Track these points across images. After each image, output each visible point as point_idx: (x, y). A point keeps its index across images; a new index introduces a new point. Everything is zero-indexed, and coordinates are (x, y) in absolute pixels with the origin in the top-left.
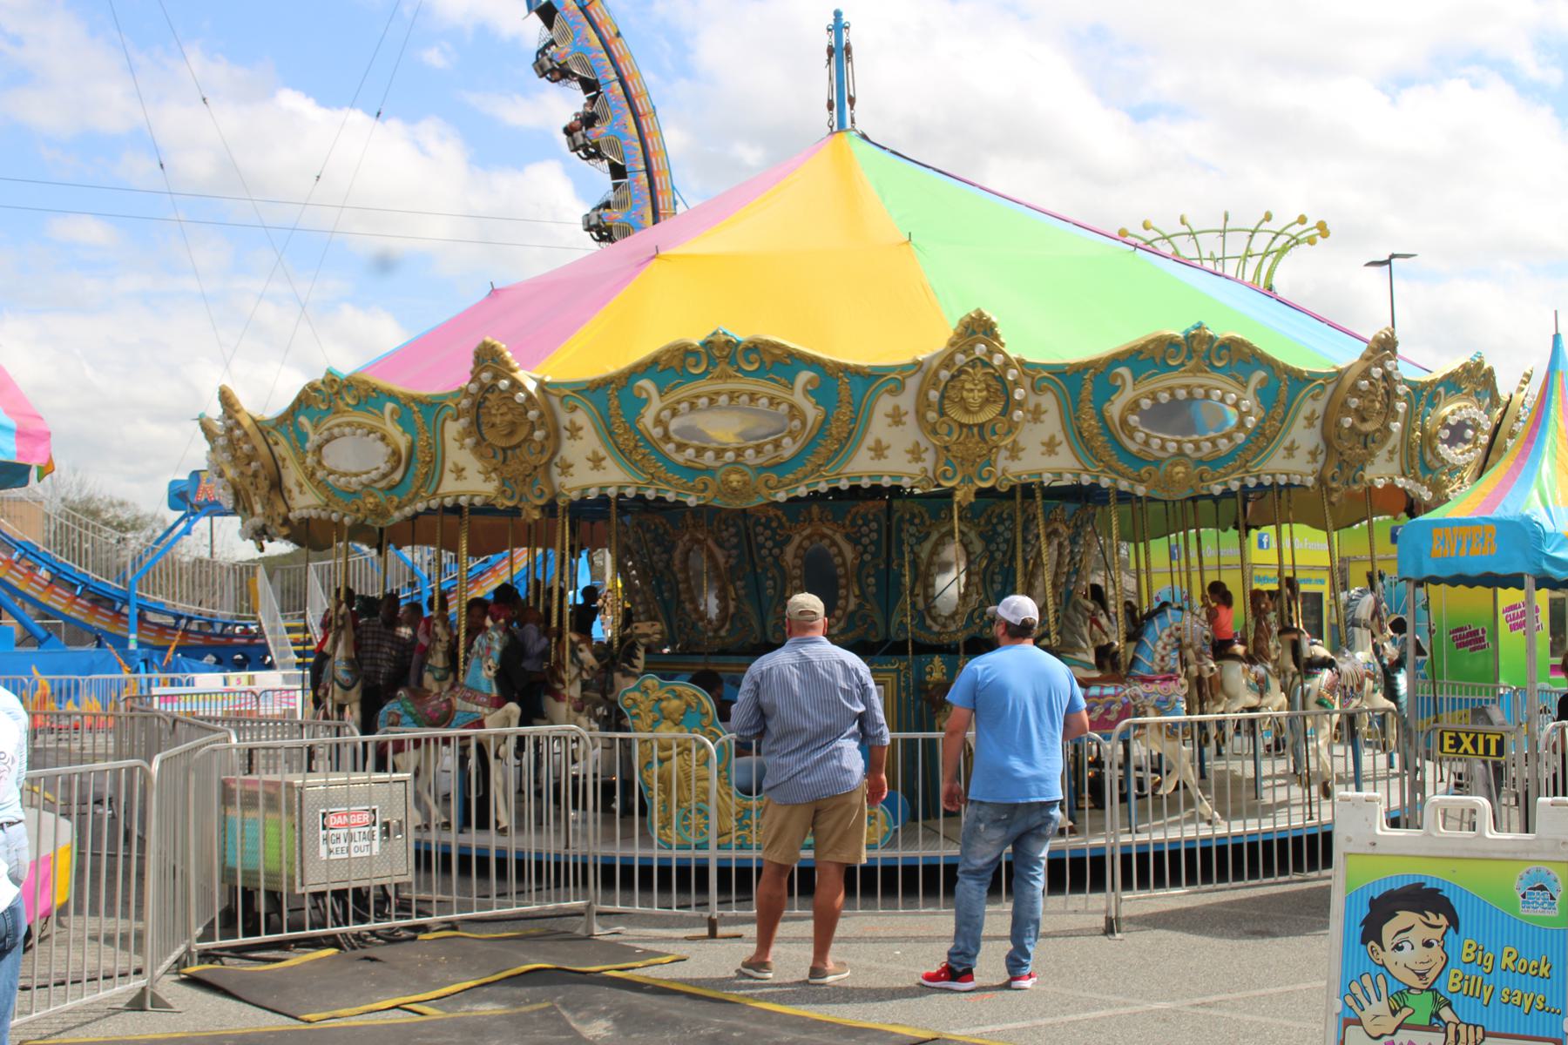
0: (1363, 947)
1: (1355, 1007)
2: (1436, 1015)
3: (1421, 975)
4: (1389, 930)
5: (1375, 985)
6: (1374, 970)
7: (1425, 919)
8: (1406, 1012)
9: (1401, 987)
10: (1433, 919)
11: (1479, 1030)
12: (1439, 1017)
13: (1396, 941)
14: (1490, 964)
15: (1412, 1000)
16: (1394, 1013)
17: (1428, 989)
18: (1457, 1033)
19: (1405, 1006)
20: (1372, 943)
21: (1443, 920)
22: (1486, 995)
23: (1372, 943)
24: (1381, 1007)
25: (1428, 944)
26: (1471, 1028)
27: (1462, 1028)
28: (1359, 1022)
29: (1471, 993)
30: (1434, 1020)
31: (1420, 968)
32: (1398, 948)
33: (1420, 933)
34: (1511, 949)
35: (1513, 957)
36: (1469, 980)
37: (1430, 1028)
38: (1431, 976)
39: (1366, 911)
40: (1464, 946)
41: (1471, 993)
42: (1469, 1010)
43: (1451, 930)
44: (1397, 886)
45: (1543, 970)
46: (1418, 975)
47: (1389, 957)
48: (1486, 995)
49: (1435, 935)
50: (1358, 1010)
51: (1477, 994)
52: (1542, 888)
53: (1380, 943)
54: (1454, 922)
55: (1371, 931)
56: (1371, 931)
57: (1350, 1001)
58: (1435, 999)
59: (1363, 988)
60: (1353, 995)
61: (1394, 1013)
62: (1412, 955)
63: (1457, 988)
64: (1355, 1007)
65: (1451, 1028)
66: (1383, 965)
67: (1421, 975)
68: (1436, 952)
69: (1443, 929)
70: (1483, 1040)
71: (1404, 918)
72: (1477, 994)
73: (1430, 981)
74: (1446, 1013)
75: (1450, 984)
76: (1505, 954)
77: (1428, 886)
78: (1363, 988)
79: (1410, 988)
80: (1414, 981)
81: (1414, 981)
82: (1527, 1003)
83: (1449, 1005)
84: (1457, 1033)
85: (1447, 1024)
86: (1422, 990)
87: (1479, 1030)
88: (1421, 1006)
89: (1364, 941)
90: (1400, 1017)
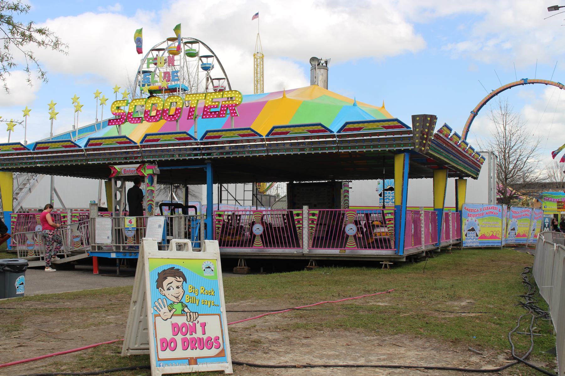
0: (157, 289)
1: (157, 310)
2: (183, 310)
3: (177, 298)
4: (165, 283)
5: (163, 302)
6: (163, 297)
7: (176, 279)
8: (174, 310)
9: (171, 302)
11: (197, 314)
12: (184, 311)
13: (168, 287)
14: (197, 292)
15: (175, 306)
16: (170, 311)
17: (180, 302)
18: (190, 315)
19: (173, 308)
20: (160, 288)
21: (181, 279)
22: (197, 302)
23: (160, 288)
24: (166, 309)
25: (178, 287)
26: (194, 313)
27: (191, 314)
28: (159, 315)
29: (193, 302)
30: (183, 312)
31: (177, 295)
32: (169, 289)
33: (175, 284)
34: (203, 287)
35: (204, 290)
36: (192, 298)
37: (182, 315)
38: (180, 298)
39: (157, 277)
40: (188, 287)
41: (193, 302)
42: (192, 307)
43: (184, 282)
45: (212, 293)
46: (176, 298)
47: (166, 292)
48: (197, 302)
49: (180, 284)
50: (158, 311)
51: (195, 303)
52: (209, 267)
53: (163, 288)
54: (185, 280)
55: (159, 284)
57: (156, 309)
58: (182, 305)
59: (159, 304)
60: (156, 306)
61: (170, 311)
62: (174, 291)
63: (188, 301)
64: (157, 310)
65: (188, 314)
66: (165, 295)
67: (177, 298)
69: (182, 282)
70: (198, 317)
71: (170, 279)
72: (195, 303)
73: (180, 299)
74: (186, 309)
76: (201, 289)
77: (176, 268)
78: (159, 304)
79: (174, 302)
80: (176, 300)
81: (176, 300)
82: (209, 304)
83: (187, 306)
84: (190, 315)
85: (187, 313)
86: (178, 303)
87: (197, 314)
88: (178, 307)
89: (158, 288)
90: (172, 312)
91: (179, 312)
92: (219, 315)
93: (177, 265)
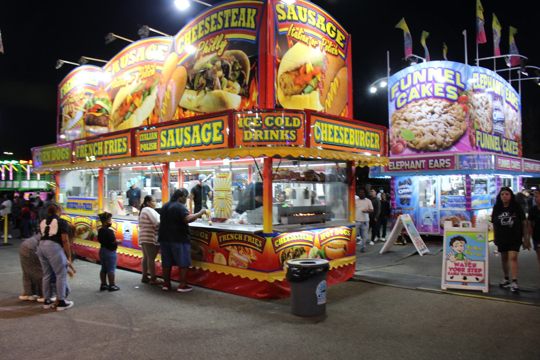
3: (460, 251)
4: (454, 244)
10: (462, 242)
24: (453, 257)
25: (461, 246)
28: (449, 259)
40: (468, 246)
44: (455, 236)
47: (454, 248)
49: (462, 244)
54: (466, 242)
55: (451, 244)
56: (451, 244)
62: (459, 248)
68: (463, 248)
71: (457, 242)
74: (464, 257)
75: (465, 253)
80: (459, 252)
81: (459, 252)
83: (465, 256)
88: (460, 256)
91: (461, 258)
92: (484, 261)
93: (462, 235)
